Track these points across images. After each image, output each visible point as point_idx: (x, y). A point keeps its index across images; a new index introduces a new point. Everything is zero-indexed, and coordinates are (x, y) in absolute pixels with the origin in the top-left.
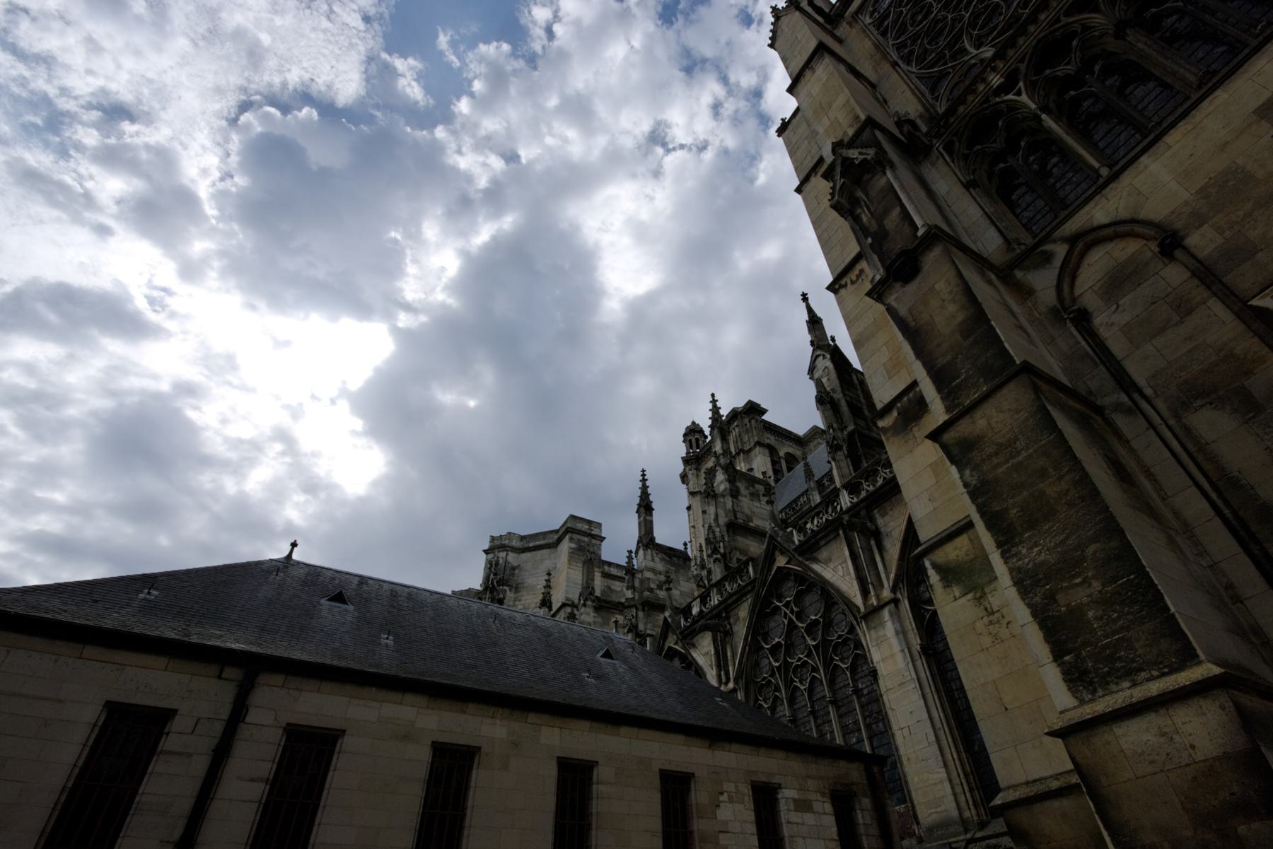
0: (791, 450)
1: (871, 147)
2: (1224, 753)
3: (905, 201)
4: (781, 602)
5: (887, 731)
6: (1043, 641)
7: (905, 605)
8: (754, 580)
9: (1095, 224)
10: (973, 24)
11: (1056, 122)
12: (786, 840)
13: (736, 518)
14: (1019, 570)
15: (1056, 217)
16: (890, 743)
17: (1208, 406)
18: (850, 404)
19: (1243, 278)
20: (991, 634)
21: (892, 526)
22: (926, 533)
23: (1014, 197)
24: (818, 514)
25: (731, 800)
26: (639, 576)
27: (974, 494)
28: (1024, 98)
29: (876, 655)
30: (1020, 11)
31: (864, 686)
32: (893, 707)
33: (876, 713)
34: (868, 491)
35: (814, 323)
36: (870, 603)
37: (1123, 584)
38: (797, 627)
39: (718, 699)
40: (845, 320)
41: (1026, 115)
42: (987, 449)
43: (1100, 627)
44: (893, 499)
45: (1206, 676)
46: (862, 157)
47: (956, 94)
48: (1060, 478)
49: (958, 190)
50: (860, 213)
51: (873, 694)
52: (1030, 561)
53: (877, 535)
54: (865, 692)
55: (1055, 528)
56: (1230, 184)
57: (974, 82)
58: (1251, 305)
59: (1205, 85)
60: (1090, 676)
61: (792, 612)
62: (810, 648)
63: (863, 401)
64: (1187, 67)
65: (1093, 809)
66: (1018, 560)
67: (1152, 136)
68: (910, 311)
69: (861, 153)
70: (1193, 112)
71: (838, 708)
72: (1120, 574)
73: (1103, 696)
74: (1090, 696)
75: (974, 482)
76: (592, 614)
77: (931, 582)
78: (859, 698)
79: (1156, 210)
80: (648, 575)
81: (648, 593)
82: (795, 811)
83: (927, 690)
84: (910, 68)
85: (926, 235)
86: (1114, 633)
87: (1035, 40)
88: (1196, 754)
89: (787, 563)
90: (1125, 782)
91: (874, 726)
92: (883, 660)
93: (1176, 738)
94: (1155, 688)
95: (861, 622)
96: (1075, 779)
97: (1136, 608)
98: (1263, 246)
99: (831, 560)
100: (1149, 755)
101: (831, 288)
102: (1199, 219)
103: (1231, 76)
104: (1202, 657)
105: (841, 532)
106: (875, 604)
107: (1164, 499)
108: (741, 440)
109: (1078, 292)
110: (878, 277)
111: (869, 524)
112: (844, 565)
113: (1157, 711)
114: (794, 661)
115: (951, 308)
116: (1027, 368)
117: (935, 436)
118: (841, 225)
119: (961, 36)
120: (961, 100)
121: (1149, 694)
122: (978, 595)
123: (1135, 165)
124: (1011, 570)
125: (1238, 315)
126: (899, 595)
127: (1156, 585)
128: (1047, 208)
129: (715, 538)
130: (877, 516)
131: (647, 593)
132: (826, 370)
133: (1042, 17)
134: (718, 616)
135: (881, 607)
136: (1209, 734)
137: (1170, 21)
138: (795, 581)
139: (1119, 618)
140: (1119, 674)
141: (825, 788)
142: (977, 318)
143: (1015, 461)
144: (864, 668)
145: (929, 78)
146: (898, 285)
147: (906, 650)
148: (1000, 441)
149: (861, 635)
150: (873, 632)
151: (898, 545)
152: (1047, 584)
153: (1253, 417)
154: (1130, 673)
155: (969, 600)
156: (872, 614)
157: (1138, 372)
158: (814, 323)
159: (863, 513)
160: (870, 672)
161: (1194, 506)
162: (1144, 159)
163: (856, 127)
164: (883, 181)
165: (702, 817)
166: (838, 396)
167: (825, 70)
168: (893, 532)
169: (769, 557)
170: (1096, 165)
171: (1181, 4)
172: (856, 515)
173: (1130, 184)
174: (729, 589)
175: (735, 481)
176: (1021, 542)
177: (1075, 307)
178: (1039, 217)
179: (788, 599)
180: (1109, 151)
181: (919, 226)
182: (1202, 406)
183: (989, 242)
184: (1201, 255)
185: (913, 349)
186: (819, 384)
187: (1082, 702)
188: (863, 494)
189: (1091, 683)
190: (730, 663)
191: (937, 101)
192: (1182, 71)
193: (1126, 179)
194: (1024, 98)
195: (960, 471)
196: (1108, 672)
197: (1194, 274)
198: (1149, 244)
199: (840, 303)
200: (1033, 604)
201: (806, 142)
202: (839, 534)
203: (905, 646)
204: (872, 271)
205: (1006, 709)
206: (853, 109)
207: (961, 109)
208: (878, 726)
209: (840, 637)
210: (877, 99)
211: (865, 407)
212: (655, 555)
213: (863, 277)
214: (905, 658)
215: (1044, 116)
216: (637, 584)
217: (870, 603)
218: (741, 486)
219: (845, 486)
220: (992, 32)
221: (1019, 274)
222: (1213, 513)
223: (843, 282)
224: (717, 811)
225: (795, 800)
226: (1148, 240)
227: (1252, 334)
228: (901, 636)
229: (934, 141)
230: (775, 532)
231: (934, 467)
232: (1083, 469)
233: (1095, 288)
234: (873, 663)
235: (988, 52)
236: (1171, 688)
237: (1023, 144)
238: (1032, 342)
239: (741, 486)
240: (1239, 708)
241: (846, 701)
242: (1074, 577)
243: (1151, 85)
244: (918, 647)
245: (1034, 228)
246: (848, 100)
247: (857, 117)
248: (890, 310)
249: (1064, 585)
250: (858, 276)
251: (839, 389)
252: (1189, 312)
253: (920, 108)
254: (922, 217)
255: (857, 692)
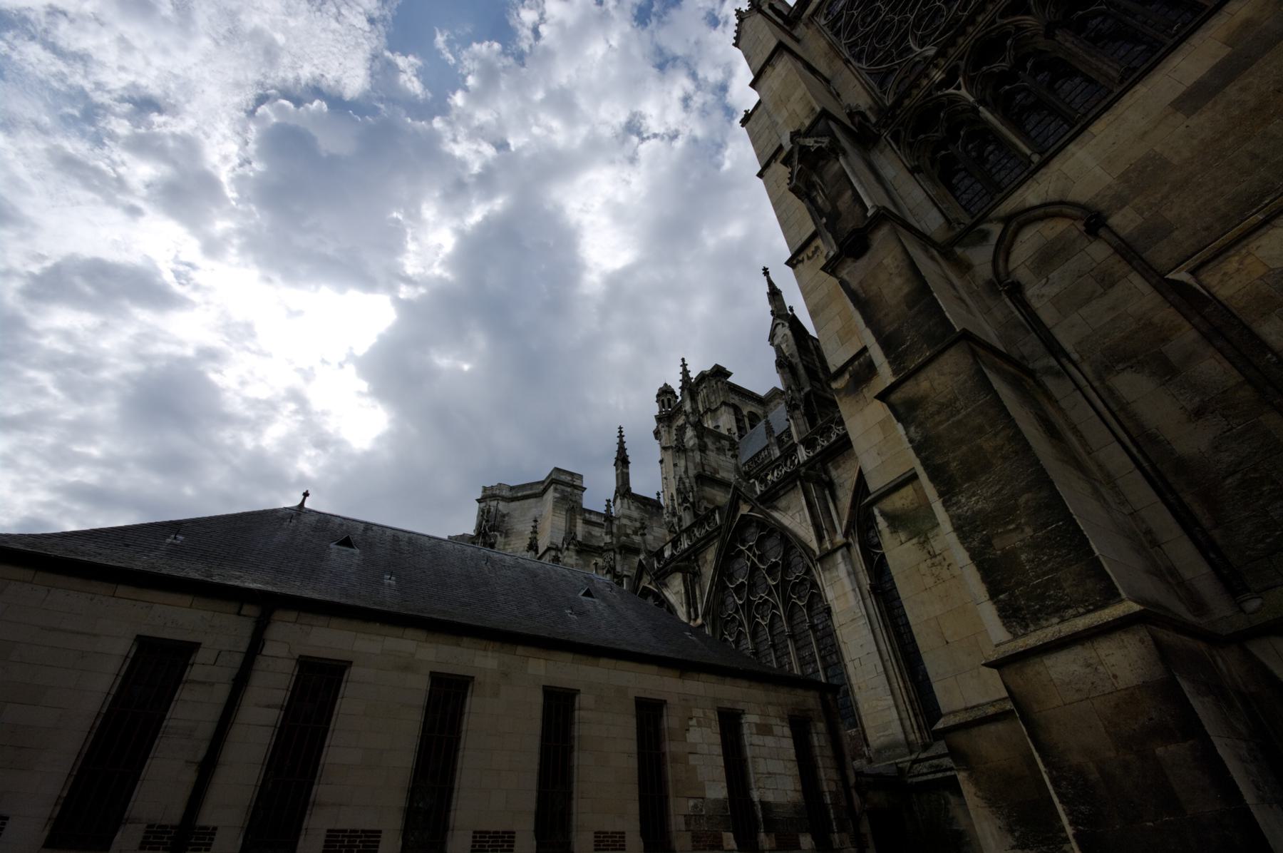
0: (753, 409)
1: (825, 136)
2: (1143, 682)
3: (856, 185)
4: (744, 546)
5: (840, 662)
6: (981, 581)
8: (720, 527)
9: (1027, 205)
10: (917, 25)
11: (992, 114)
12: (749, 760)
13: (704, 471)
14: (959, 517)
15: (992, 199)
16: (842, 673)
17: (1129, 369)
18: (806, 368)
19: (1161, 255)
20: (933, 575)
21: (845, 478)
22: (875, 484)
23: (954, 181)
24: (777, 467)
25: (699, 725)
26: (617, 522)
27: (918, 449)
28: (963, 92)
29: (830, 594)
30: (960, 14)
31: (819, 622)
32: (845, 641)
33: (831, 646)
34: (822, 446)
35: (774, 294)
36: (824, 546)
37: (1052, 530)
38: (759, 568)
39: (688, 634)
40: (802, 292)
41: (966, 107)
42: (929, 408)
43: (1032, 568)
44: (845, 453)
45: (1127, 613)
46: (818, 145)
47: (902, 88)
48: (996, 435)
49: (905, 175)
50: (815, 196)
51: (828, 629)
52: (968, 509)
53: (831, 486)
55: (991, 479)
56: (1149, 169)
57: (918, 78)
58: (1168, 279)
59: (1127, 79)
60: (1023, 612)
61: (754, 555)
63: (818, 364)
64: (1111, 64)
65: (1026, 733)
66: (958, 509)
67: (1079, 126)
68: (861, 283)
69: (816, 142)
70: (1116, 105)
71: (796, 642)
72: (1050, 521)
73: (1035, 631)
74: (1022, 631)
75: (918, 438)
76: (574, 557)
77: (880, 528)
78: (815, 632)
79: (1082, 192)
80: (625, 521)
81: (625, 538)
82: (757, 734)
83: (876, 625)
84: (860, 65)
85: (875, 215)
86: (1045, 574)
87: (974, 40)
88: (1118, 683)
89: (749, 512)
90: (1054, 708)
91: (828, 658)
92: (836, 598)
93: (1101, 669)
94: (1081, 623)
95: (817, 564)
96: (1009, 706)
97: (1064, 551)
98: (1178, 226)
99: (789, 508)
100: (1076, 683)
101: (789, 263)
102: (1121, 201)
103: (1149, 72)
104: (1124, 595)
105: (798, 483)
106: (829, 548)
107: (1089, 454)
108: (709, 400)
109: (1011, 266)
110: (832, 254)
111: (824, 476)
112: (801, 513)
113: (1083, 645)
115: (898, 281)
116: (966, 336)
117: (883, 396)
118: (798, 207)
119: (907, 35)
120: (906, 94)
121: (1076, 629)
122: (922, 540)
123: (1063, 152)
124: (951, 517)
125: (1155, 287)
126: (851, 540)
127: (1082, 531)
128: (984, 191)
129: (685, 488)
130: (831, 468)
131: (623, 538)
132: (785, 337)
133: (980, 19)
134: (688, 558)
135: (834, 551)
136: (1130, 665)
137: (1095, 22)
138: (757, 527)
139: (1049, 560)
140: (1049, 611)
141: (784, 713)
142: (922, 290)
143: (955, 419)
144: (819, 606)
145: (879, 73)
146: (849, 261)
147: (857, 589)
148: (941, 401)
149: (817, 576)
150: (827, 573)
151: (850, 495)
152: (984, 530)
153: (1170, 379)
154: (1059, 610)
155: (914, 545)
156: (827, 556)
157: (1066, 340)
158: (774, 294)
159: (818, 465)
160: (825, 609)
161: (1116, 459)
162: (1071, 147)
163: (812, 117)
164: (836, 167)
165: (673, 740)
166: (796, 360)
167: (784, 66)
168: (845, 483)
169: (734, 506)
170: (1028, 152)
171: (1105, 7)
172: (813, 468)
173: (1059, 169)
174: (697, 534)
175: (703, 436)
176: (961, 492)
177: (1009, 281)
178: (976, 199)
179: (751, 543)
180: (1040, 140)
181: (869, 208)
182: (1123, 370)
183: (932, 222)
184: (1123, 234)
185: (864, 318)
186: (778, 349)
187: (1016, 636)
188: (819, 449)
189: (1023, 619)
190: (698, 601)
191: (885, 94)
192: (1105, 67)
193: (1055, 165)
194: (963, 92)
195: (906, 428)
196: (1039, 609)
197: (1117, 251)
198: (1076, 223)
199: (797, 276)
200: (971, 548)
201: (767, 131)
202: (796, 485)
203: (855, 586)
204: (826, 248)
205: (947, 643)
206: (809, 102)
207: (907, 102)
208: (831, 658)
209: (797, 577)
210: (831, 93)
211: (820, 370)
212: (631, 503)
213: (818, 253)
214: (856, 596)
215: (981, 108)
216: (615, 530)
217: (824, 546)
218: (709, 441)
219: (802, 442)
220: (934, 33)
221: (959, 251)
222: (1133, 466)
223: (800, 258)
224: (687, 735)
225: (757, 725)
226: (1075, 220)
227: (1169, 305)
228: (852, 577)
229: (883, 131)
230: (739, 483)
231: (883, 424)
232: (1016, 426)
233: (1027, 263)
234: (827, 601)
235: (931, 51)
236: (1096, 624)
237: (962, 133)
238: (969, 311)
239: (709, 441)
240: (1158, 643)
241: (803, 635)
242: (1008, 523)
243: (1077, 80)
244: (868, 586)
245: (972, 209)
246: (805, 94)
247: (813, 109)
248: (843, 283)
249: (999, 531)
250: (814, 253)
251: (796, 354)
252: (1112, 285)
253: (870, 101)
254: (871, 199)
255: (813, 627)
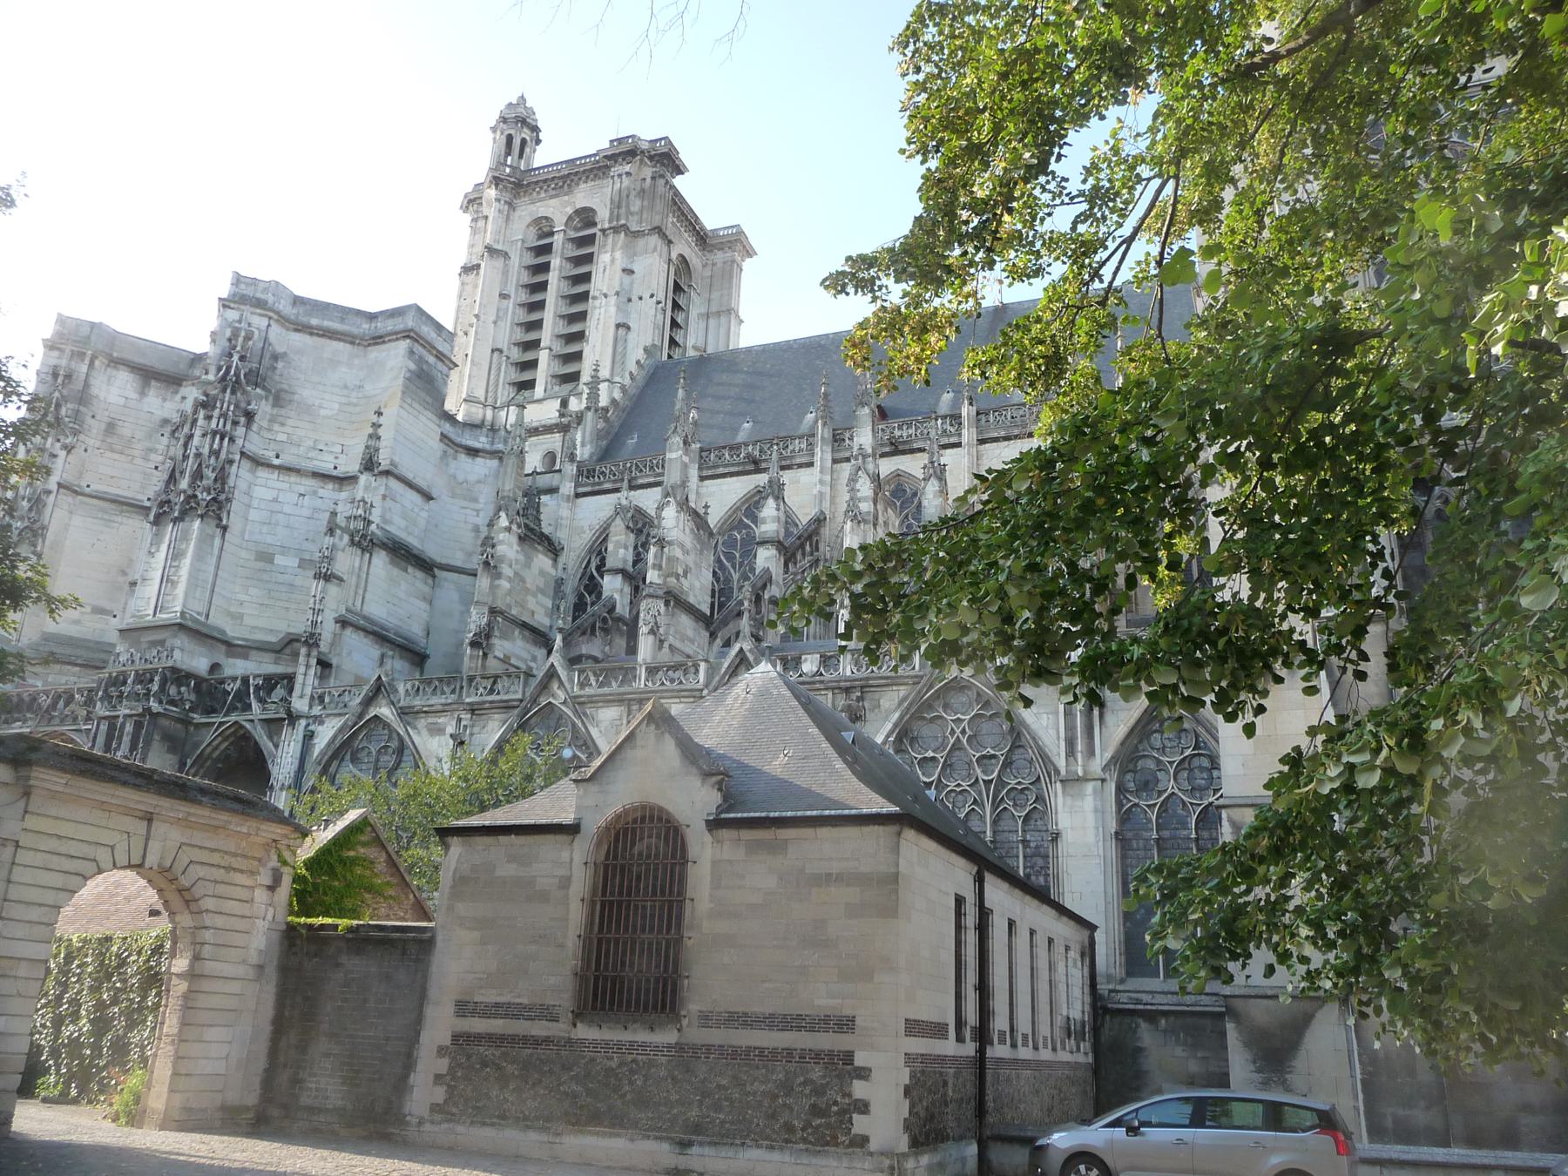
7: (1112, 787)
54: (1032, 845)
62: (977, 779)
78: (1025, 847)
114: (952, 786)
135: (1085, 779)
228: (1099, 814)
